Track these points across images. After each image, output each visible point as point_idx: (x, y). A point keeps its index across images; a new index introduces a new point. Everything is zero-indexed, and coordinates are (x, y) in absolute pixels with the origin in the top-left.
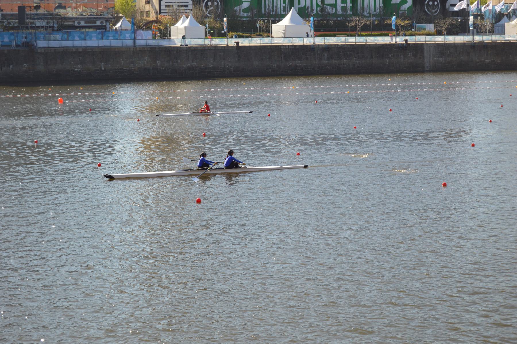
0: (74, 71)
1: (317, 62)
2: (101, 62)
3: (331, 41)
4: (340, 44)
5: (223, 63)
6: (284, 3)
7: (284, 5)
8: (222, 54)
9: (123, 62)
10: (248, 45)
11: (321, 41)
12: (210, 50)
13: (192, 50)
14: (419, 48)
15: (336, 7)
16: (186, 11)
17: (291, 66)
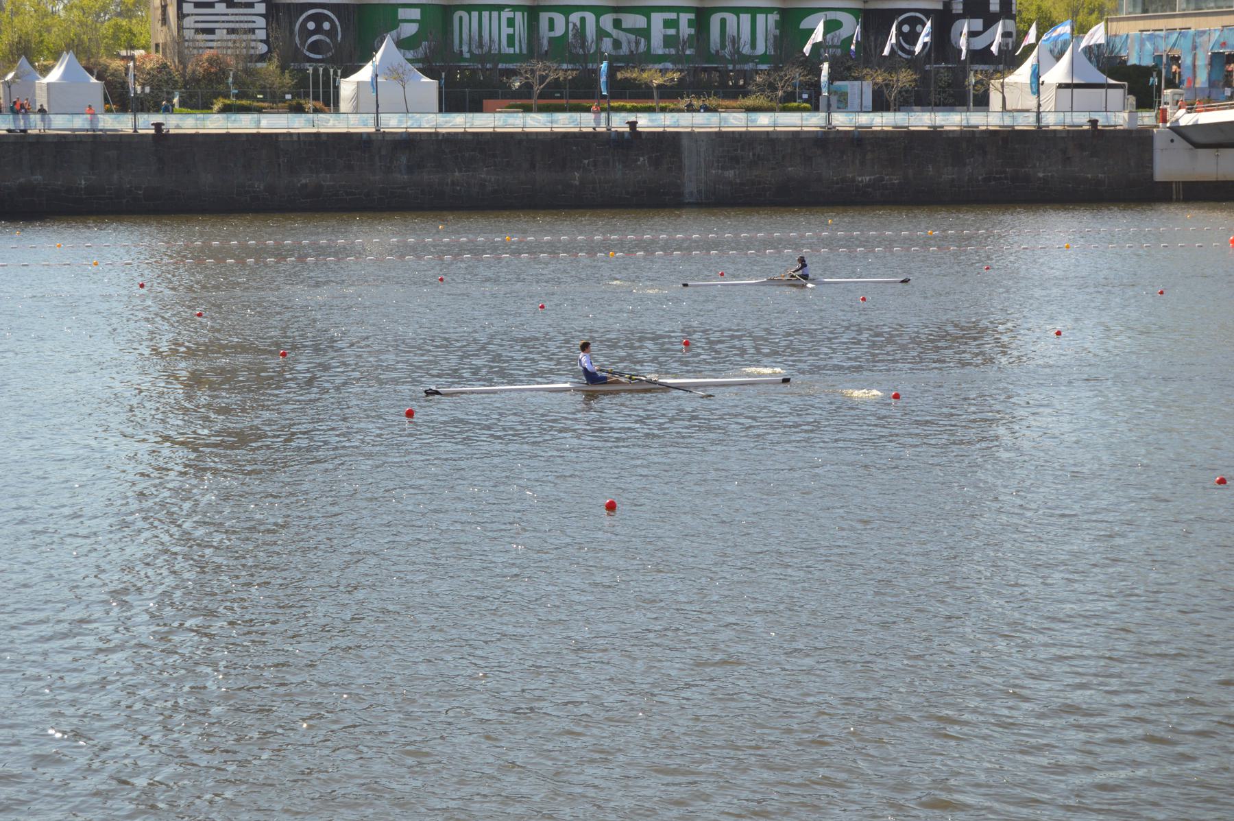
1: (377, 178)
3: (921, 120)
4: (444, 131)
5: (115, 177)
6: (508, 26)
7: (510, 31)
10: (193, 131)
11: (458, 122)
12: (80, 142)
13: (31, 144)
14: (667, 143)
15: (648, 38)
16: (211, 44)
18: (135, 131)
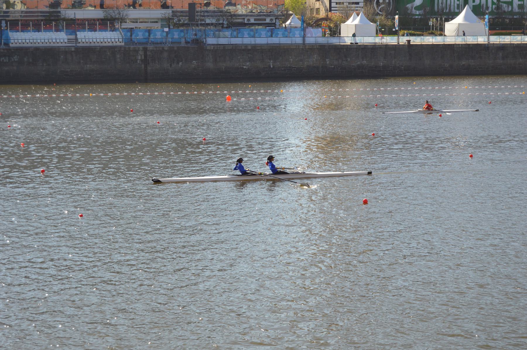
0: (243, 68)
1: (491, 62)
2: (270, 60)
3: (507, 40)
4: (516, 43)
5: (393, 61)
7: (458, 2)
8: (393, 52)
9: (292, 60)
10: (420, 43)
11: (496, 40)
12: (381, 48)
13: (362, 49)
16: (357, 9)
17: (464, 65)
18: (398, 43)
